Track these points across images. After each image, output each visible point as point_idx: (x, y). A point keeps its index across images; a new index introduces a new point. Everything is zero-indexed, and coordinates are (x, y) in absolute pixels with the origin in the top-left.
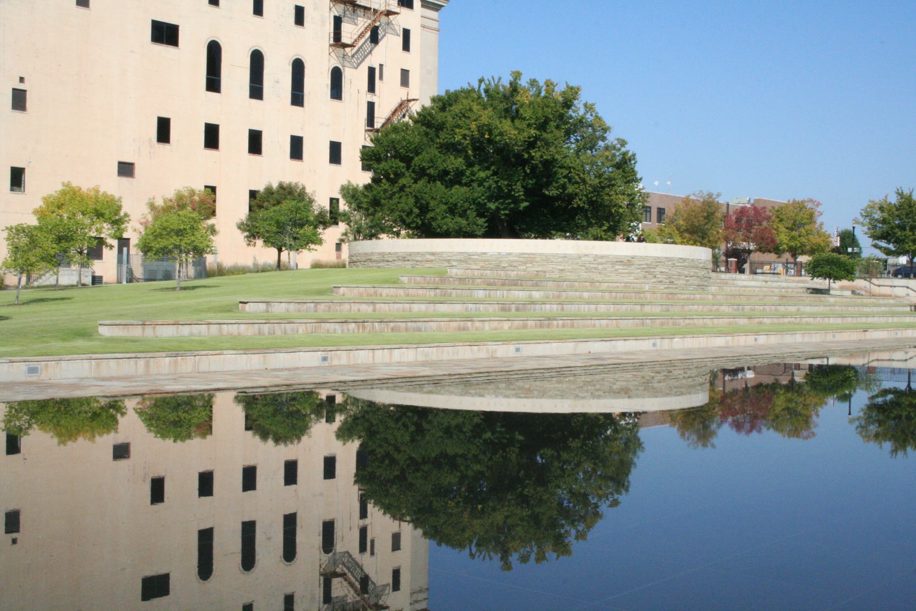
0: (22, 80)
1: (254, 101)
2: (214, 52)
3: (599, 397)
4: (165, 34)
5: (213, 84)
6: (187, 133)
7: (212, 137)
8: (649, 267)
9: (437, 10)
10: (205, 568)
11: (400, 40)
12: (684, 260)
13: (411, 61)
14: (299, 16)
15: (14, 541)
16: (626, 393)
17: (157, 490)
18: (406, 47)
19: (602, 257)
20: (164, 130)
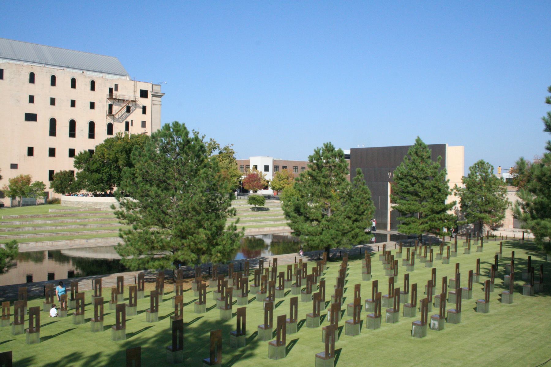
1: (71, 138)
2: (53, 122)
4: (31, 117)
5: (53, 132)
6: (41, 152)
7: (52, 152)
11: (142, 110)
13: (147, 118)
14: (92, 106)
18: (144, 112)
20: (31, 151)
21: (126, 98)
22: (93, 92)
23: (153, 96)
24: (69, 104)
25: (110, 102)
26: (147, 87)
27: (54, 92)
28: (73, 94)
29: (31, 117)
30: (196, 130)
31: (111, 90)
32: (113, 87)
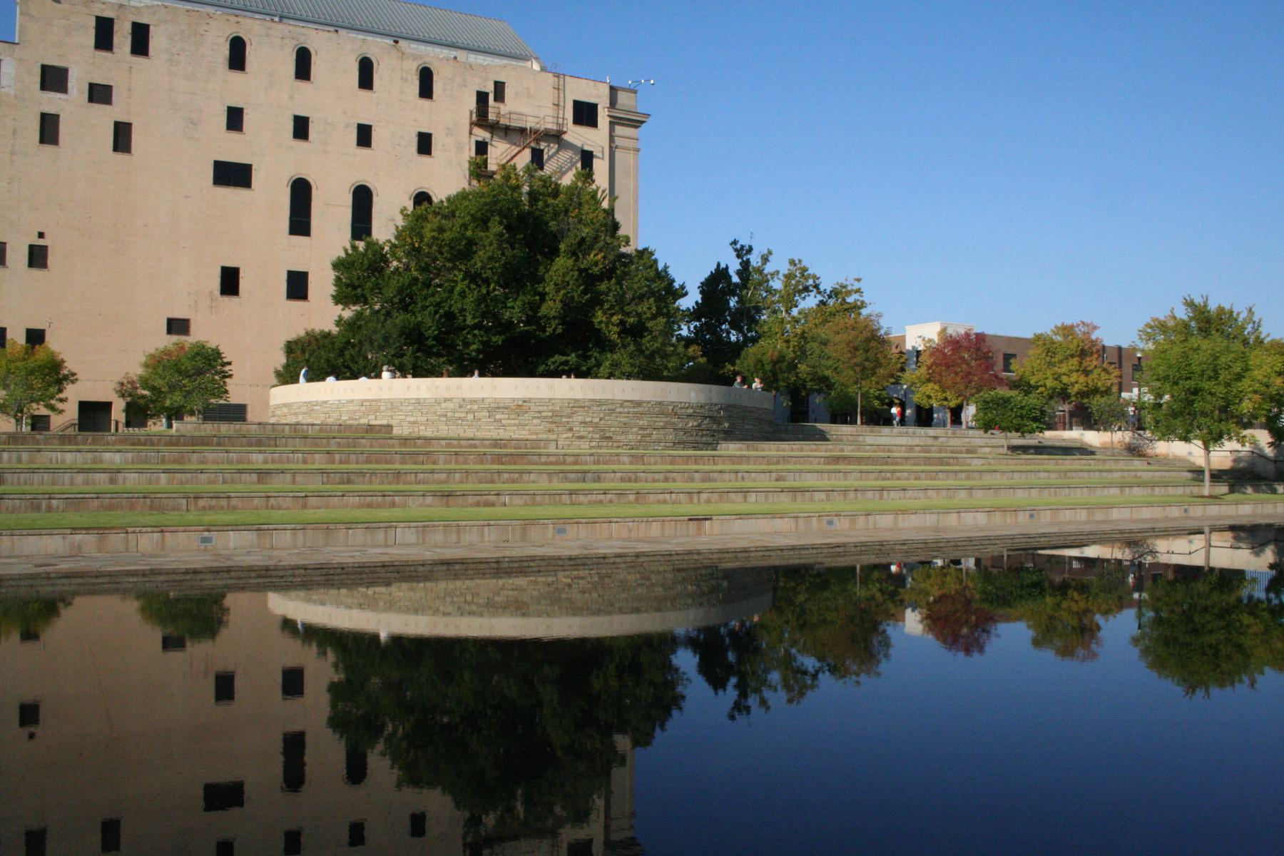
0: (41, 235)
2: (301, 192)
3: (471, 613)
4: (233, 175)
8: (558, 415)
9: (637, 127)
10: (294, 777)
12: (638, 404)
14: (425, 144)
15: (32, 736)
16: (518, 608)
17: (225, 687)
19: (473, 401)
20: (230, 281)
21: (530, 124)
22: (425, 103)
23: (615, 122)
24: (353, 135)
25: (482, 134)
26: (596, 94)
27: (304, 99)
28: (365, 107)
29: (233, 175)
30: (744, 241)
31: (482, 98)
32: (490, 88)
